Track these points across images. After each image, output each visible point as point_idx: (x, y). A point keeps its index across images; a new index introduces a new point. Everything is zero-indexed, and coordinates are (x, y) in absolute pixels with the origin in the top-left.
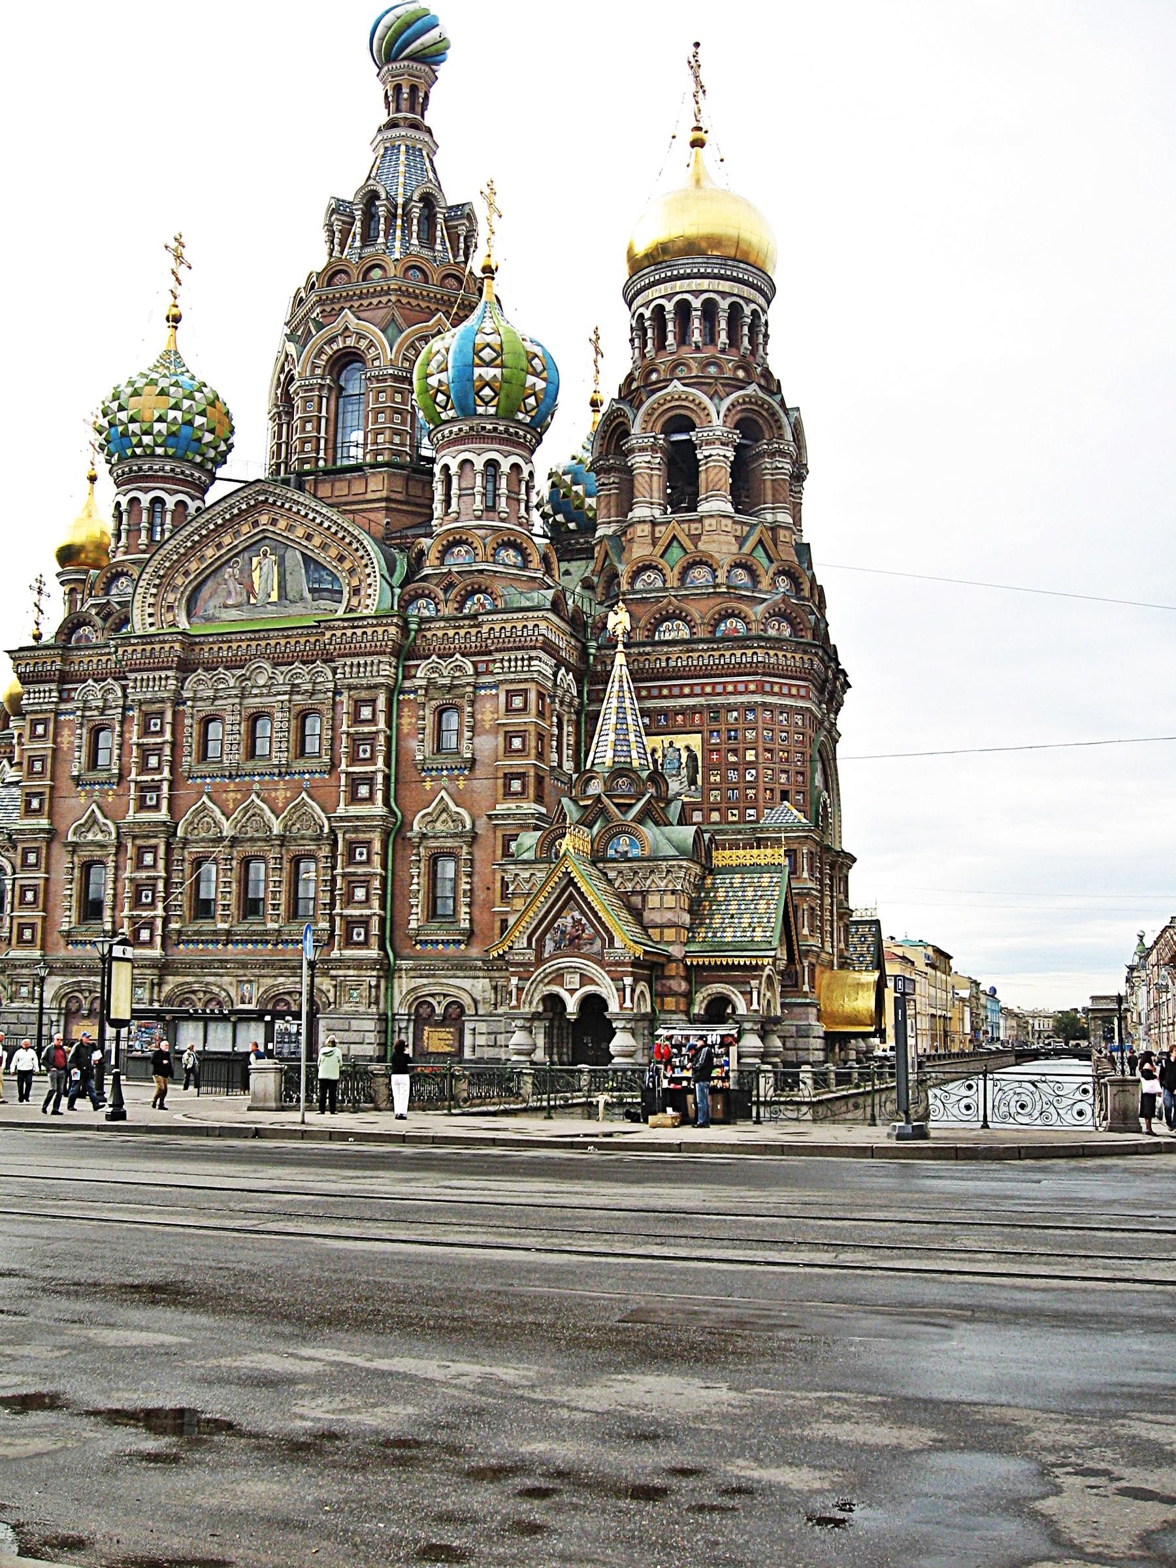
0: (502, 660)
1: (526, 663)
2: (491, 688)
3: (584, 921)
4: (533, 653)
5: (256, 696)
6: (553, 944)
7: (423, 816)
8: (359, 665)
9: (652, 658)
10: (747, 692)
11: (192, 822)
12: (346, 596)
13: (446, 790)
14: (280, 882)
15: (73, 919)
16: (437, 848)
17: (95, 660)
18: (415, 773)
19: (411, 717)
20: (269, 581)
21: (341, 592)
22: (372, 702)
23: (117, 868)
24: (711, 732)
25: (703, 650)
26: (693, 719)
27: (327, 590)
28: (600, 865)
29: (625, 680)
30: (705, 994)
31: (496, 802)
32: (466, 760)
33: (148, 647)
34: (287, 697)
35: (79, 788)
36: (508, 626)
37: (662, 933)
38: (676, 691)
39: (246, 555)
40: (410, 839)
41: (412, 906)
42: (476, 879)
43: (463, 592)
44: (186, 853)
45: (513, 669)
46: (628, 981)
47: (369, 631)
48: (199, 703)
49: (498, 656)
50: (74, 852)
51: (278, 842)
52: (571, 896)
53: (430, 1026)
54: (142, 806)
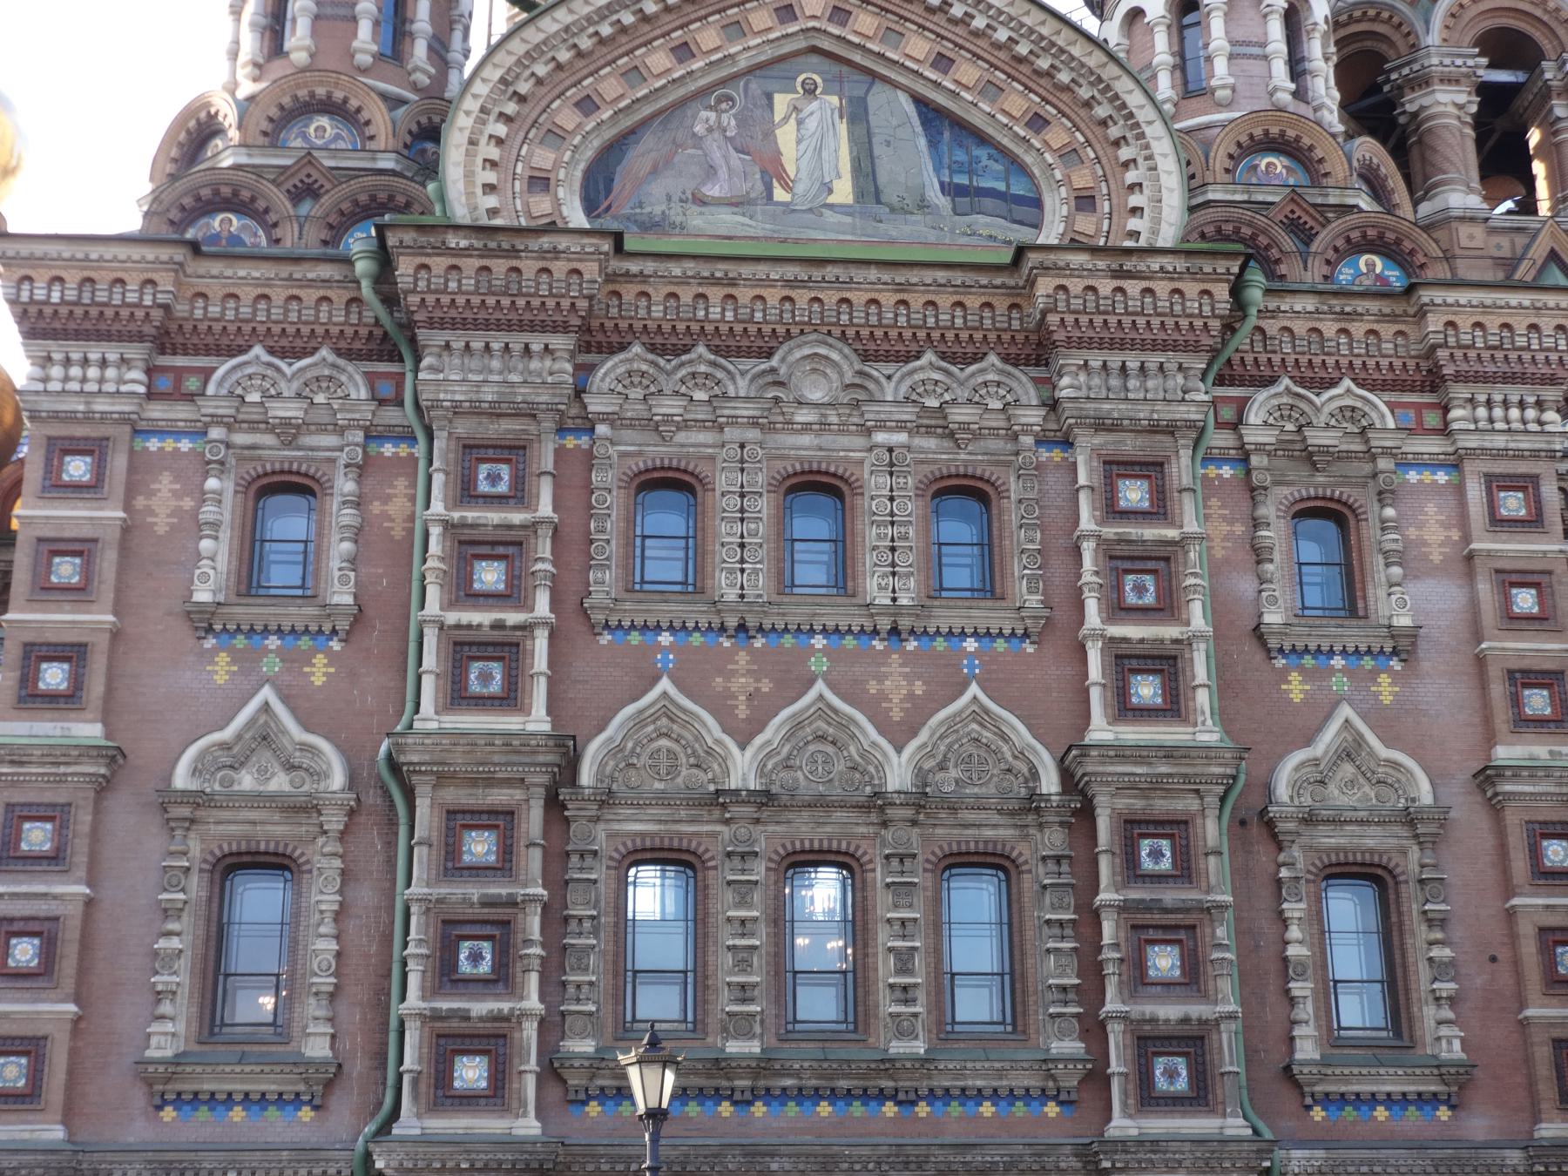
2: (1435, 466)
5: (806, 428)
7: (1297, 769)
8: (1123, 367)
11: (620, 749)
12: (1056, 208)
14: (915, 920)
15: (180, 1027)
16: (1337, 850)
17: (278, 295)
18: (1259, 656)
19: (1231, 522)
20: (825, 154)
21: (1037, 203)
22: (1152, 469)
23: (344, 873)
27: (991, 193)
31: (1490, 740)
32: (1392, 632)
33: (500, 266)
34: (901, 438)
35: (210, 642)
36: (1493, 323)
39: (755, 87)
40: (1270, 825)
41: (1292, 1002)
42: (1457, 932)
43: (1340, 243)
44: (602, 836)
45: (1500, 425)
47: (1162, 288)
48: (627, 434)
49: (1460, 392)
50: (192, 821)
51: (908, 813)
54: (458, 697)
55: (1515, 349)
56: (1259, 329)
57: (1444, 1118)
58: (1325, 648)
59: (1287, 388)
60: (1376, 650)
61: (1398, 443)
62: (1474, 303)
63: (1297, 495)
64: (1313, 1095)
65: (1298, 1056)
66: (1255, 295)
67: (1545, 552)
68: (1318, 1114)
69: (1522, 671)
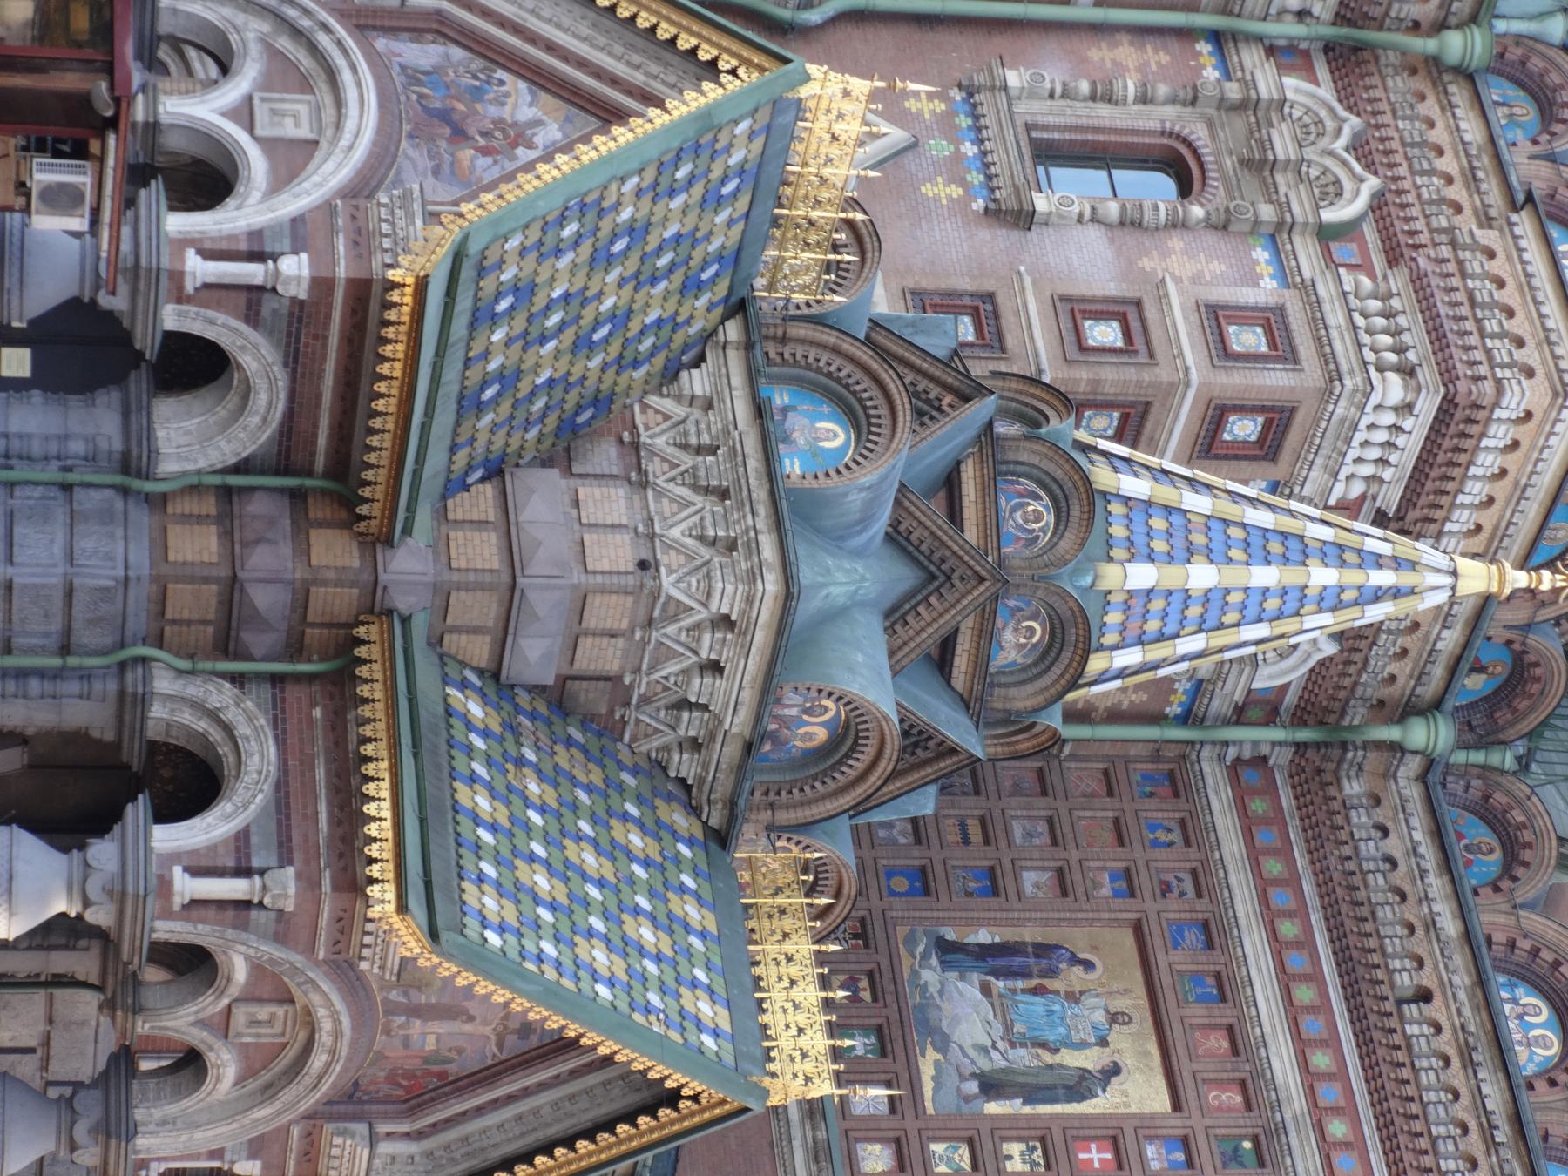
0: (1386, 297)
1: (1392, 357)
4: (1427, 375)
9: (1419, 945)
13: (913, 146)
19: (1142, 68)
24: (1185, 1144)
25: (1479, 1098)
26: (1220, 1084)
28: (733, 331)
29: (1406, 579)
30: (231, 715)
36: (1509, 296)
37: (481, 524)
38: (1312, 1026)
45: (1360, 321)
46: (295, 269)
49: (1398, 281)
55: (1478, 321)
56: (1423, 98)
59: (1344, 120)
61: (1300, 219)
62: (1529, 269)
63: (1199, 143)
66: (1454, 44)
67: (1181, 354)
69: (996, 314)
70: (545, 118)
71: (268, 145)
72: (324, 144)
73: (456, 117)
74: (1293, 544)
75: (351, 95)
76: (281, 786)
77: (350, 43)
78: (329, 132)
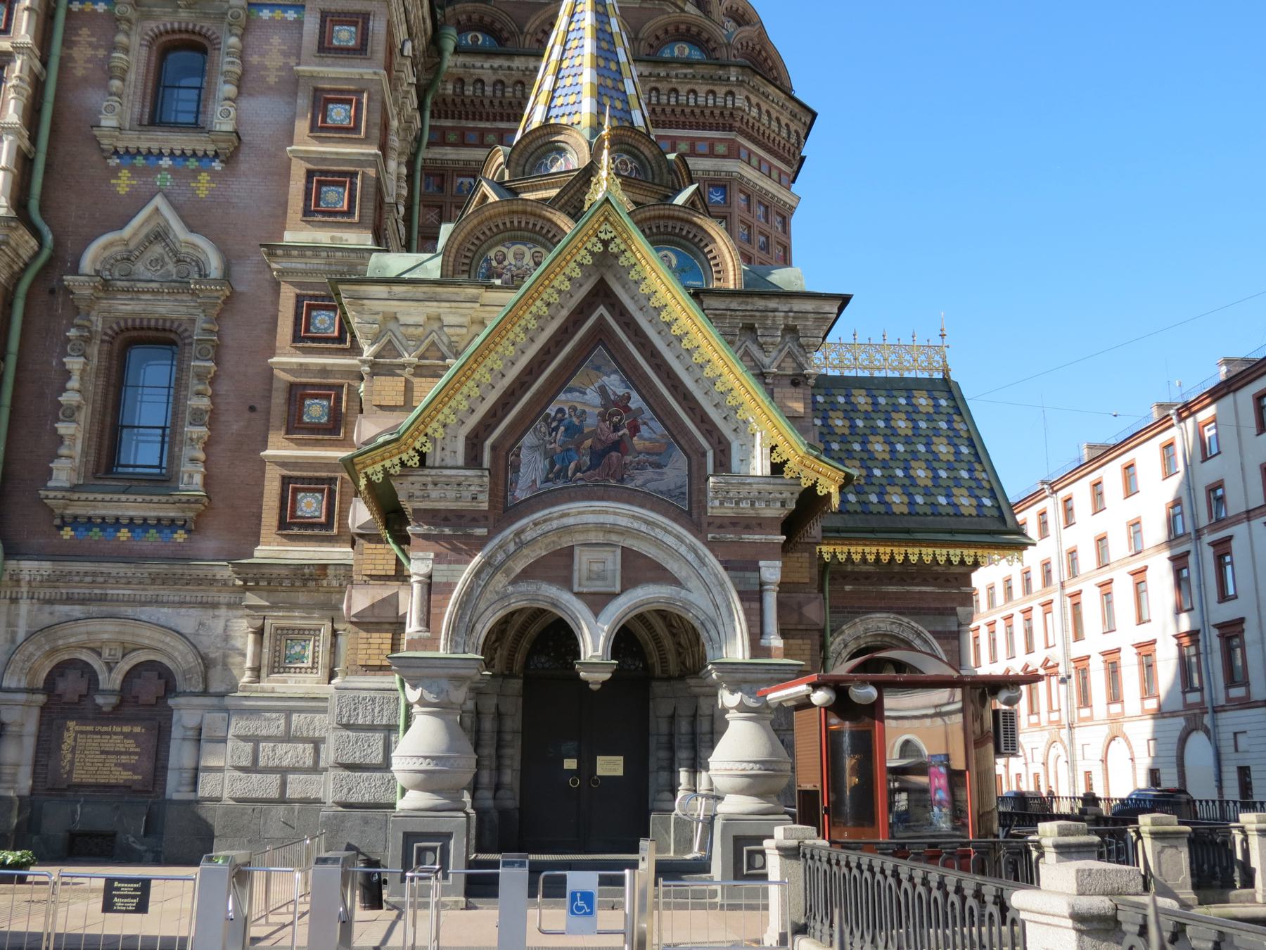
3: (636, 402)
6: (541, 464)
7: (105, 248)
10: (712, 154)
13: (166, 196)
19: (95, 48)
42: (224, 387)
52: (601, 335)
53: (82, 719)
57: (181, 540)
58: (155, 151)
60: (200, 154)
64: (62, 517)
65: (50, 484)
68: (67, 533)
70: (596, 385)
71: (629, 582)
72: (629, 543)
73: (599, 446)
74: (601, 36)
75: (591, 519)
76: (900, 612)
77: (537, 516)
78: (614, 538)
